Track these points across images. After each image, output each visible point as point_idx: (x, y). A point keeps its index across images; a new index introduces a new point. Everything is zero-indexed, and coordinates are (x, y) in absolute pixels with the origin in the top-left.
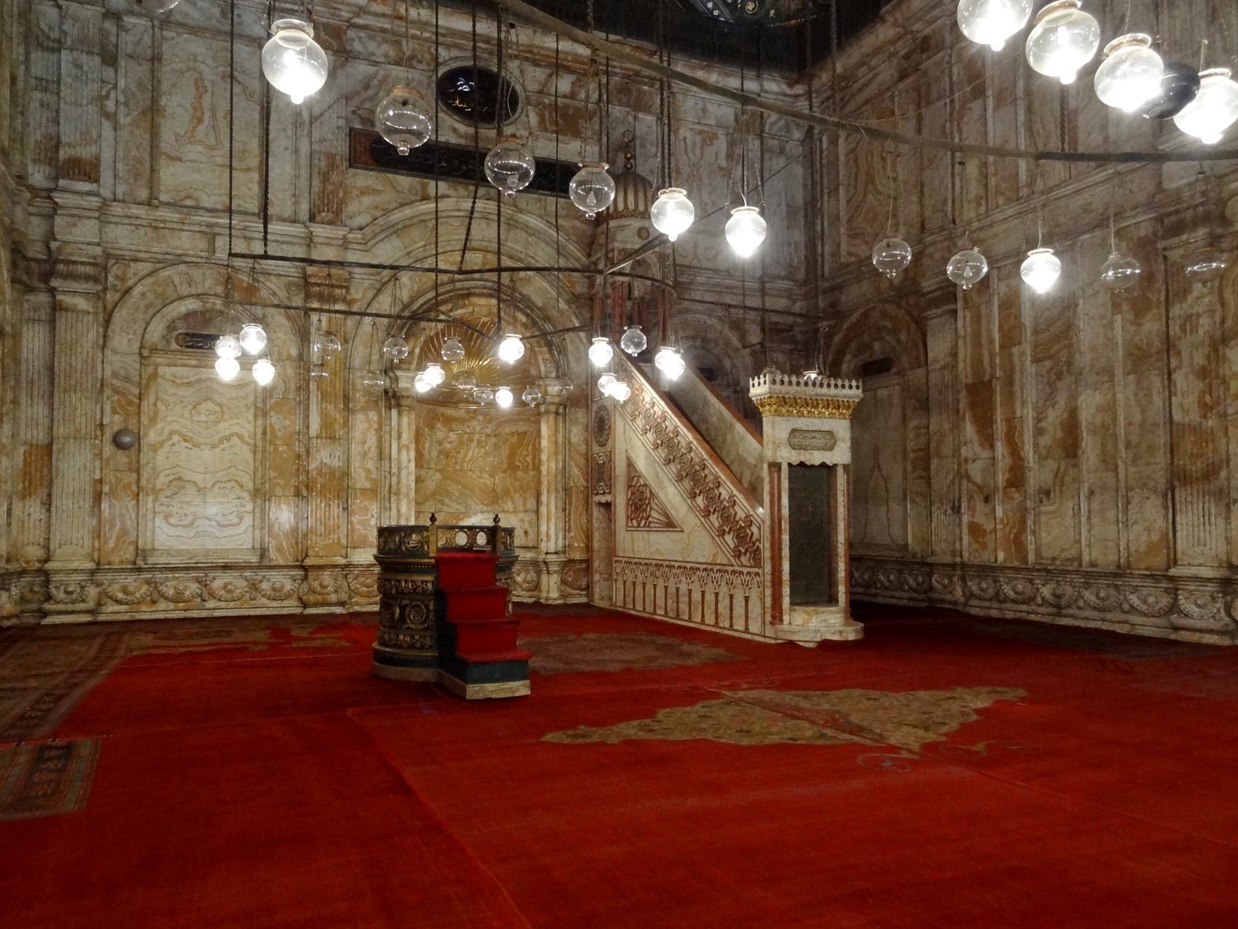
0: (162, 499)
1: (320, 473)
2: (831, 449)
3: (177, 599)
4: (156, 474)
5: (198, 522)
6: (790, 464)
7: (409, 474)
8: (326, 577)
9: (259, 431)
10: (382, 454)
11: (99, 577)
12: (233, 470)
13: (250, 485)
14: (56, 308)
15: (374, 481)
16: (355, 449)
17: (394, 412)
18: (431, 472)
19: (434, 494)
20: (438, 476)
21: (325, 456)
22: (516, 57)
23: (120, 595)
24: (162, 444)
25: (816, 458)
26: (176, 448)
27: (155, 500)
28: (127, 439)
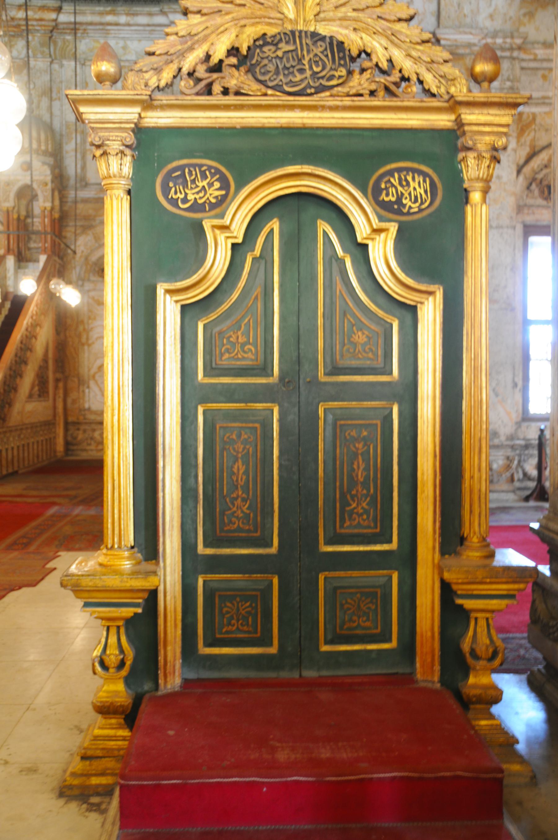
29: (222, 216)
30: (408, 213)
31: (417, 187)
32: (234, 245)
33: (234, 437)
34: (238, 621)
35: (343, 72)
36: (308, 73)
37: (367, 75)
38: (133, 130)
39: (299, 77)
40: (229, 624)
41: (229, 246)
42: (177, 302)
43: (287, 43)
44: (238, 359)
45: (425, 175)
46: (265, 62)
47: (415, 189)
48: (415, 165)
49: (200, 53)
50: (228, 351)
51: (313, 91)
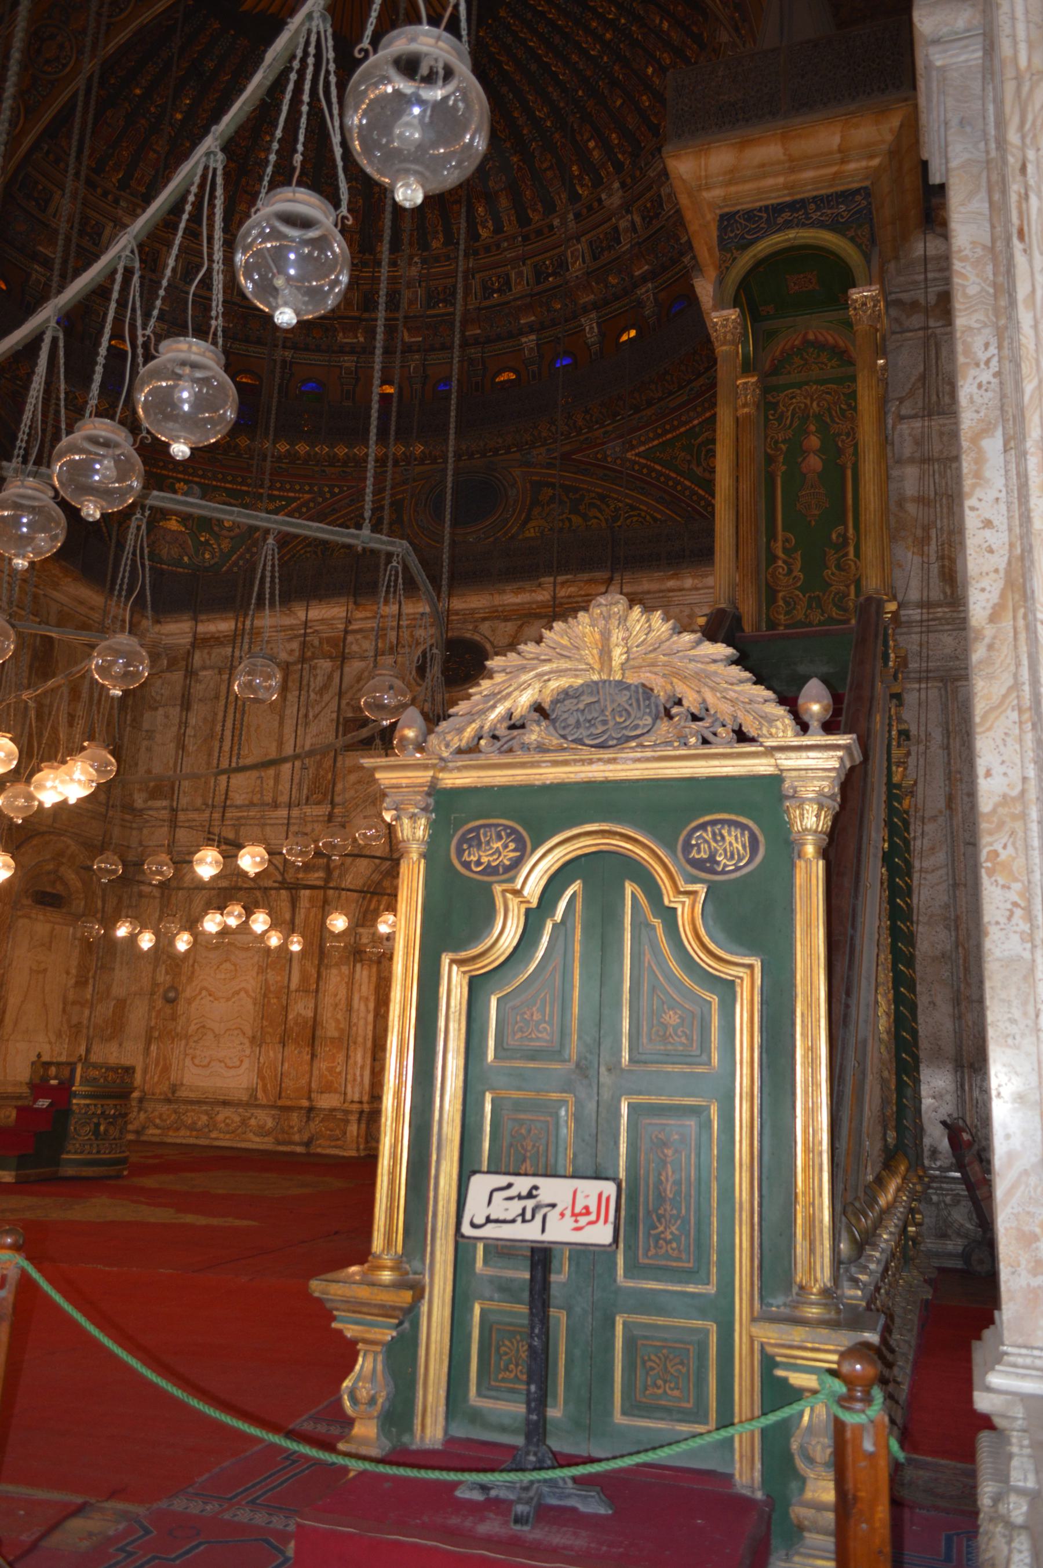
0: (193, 1045)
1: (296, 1024)
3: (192, 1128)
5: (213, 1064)
7: (366, 1024)
8: (295, 1118)
10: (350, 1008)
11: (145, 1104)
13: (249, 1033)
14: (141, 895)
15: (342, 1031)
16: (327, 1001)
17: (358, 966)
21: (302, 1008)
22: (484, 619)
23: (158, 1121)
24: (195, 998)
28: (172, 995)
29: (512, 880)
30: (723, 872)
31: (735, 841)
32: (528, 911)
33: (523, 1131)
34: (517, 1365)
36: (611, 723)
39: (601, 729)
40: (507, 1369)
41: (523, 910)
42: (464, 973)
43: (591, 694)
44: (532, 1040)
45: (743, 827)
46: (565, 716)
47: (731, 844)
48: (733, 817)
49: (500, 710)
50: (521, 1030)
51: (615, 742)
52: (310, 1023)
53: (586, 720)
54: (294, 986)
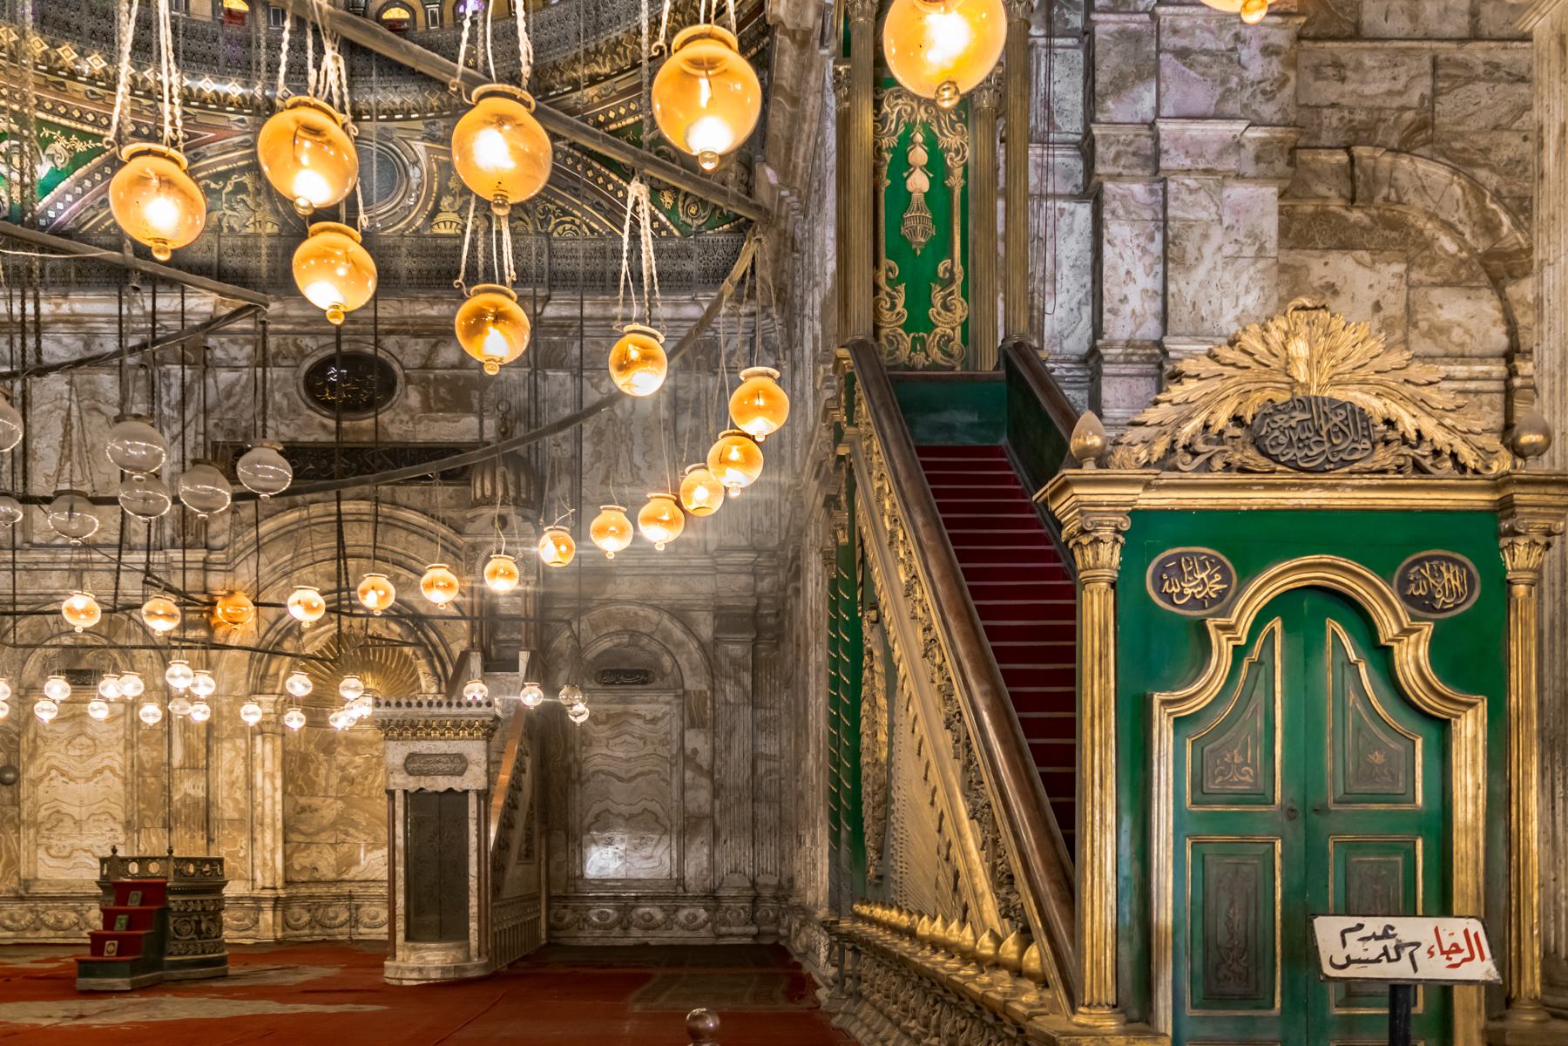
1: (184, 804)
2: (461, 773)
4: (36, 806)
6: (405, 792)
7: (274, 804)
9: (129, 763)
10: (250, 786)
12: (106, 803)
13: (121, 817)
15: (242, 811)
16: (221, 778)
18: (330, 800)
19: (333, 825)
20: (340, 804)
21: (189, 787)
25: (441, 783)
26: (54, 783)
27: (38, 832)
35: (1369, 445)
37: (1394, 447)
38: (1129, 514)
52: (202, 804)
53: (1300, 440)
54: (177, 759)
